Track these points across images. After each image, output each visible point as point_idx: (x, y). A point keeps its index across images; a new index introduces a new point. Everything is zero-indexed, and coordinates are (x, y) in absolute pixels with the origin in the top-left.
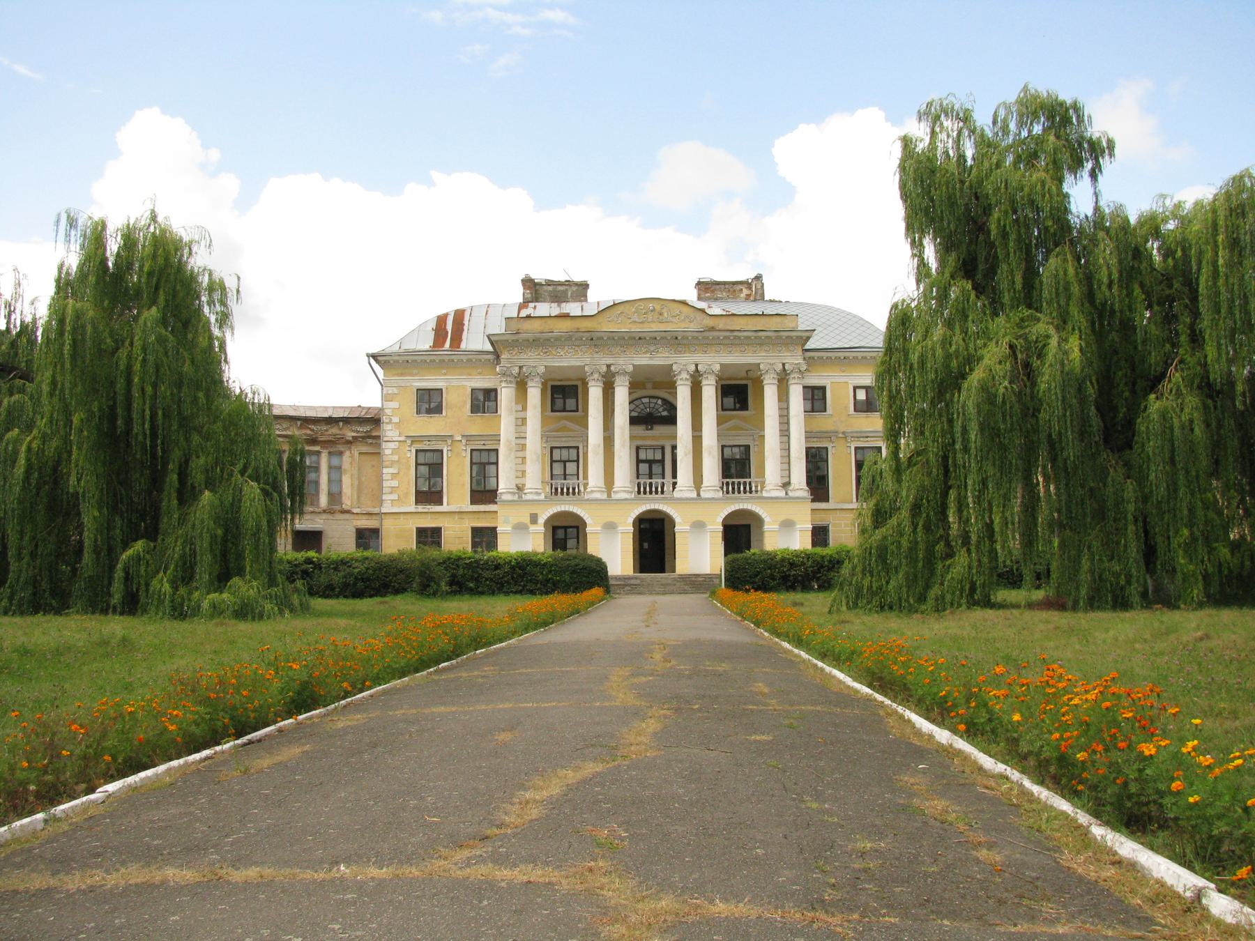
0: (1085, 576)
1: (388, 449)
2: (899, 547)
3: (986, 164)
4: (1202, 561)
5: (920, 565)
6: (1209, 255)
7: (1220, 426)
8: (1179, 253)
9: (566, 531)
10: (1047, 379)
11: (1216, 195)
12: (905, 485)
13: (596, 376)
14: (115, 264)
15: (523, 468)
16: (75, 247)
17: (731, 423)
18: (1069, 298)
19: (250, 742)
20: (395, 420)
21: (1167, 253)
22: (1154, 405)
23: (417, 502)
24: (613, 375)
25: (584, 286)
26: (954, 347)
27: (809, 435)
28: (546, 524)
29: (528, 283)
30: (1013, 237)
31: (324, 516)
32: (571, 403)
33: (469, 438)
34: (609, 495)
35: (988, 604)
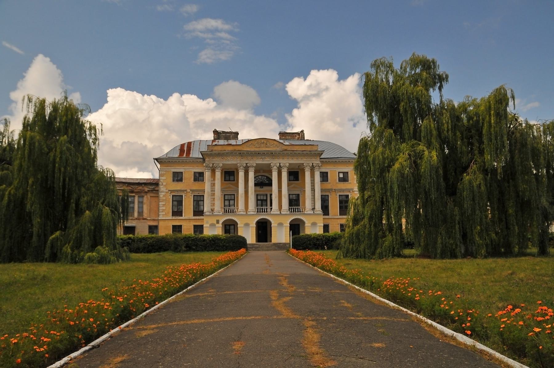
0: (439, 245)
1: (161, 195)
2: (364, 233)
3: (399, 84)
4: (485, 239)
5: (373, 240)
6: (487, 119)
7: (491, 186)
8: (475, 119)
9: (230, 226)
10: (424, 167)
11: (489, 96)
12: (366, 209)
13: (242, 168)
14: (49, 118)
15: (213, 202)
16: (32, 109)
17: (293, 185)
18: (431, 136)
19: (94, 347)
20: (164, 184)
21: (470, 118)
22: (466, 178)
24: (248, 167)
26: (386, 155)
27: (322, 190)
28: (222, 224)
29: (215, 132)
30: (409, 112)
31: (136, 221)
32: (232, 178)
33: (193, 191)
34: (247, 213)
35: (399, 256)
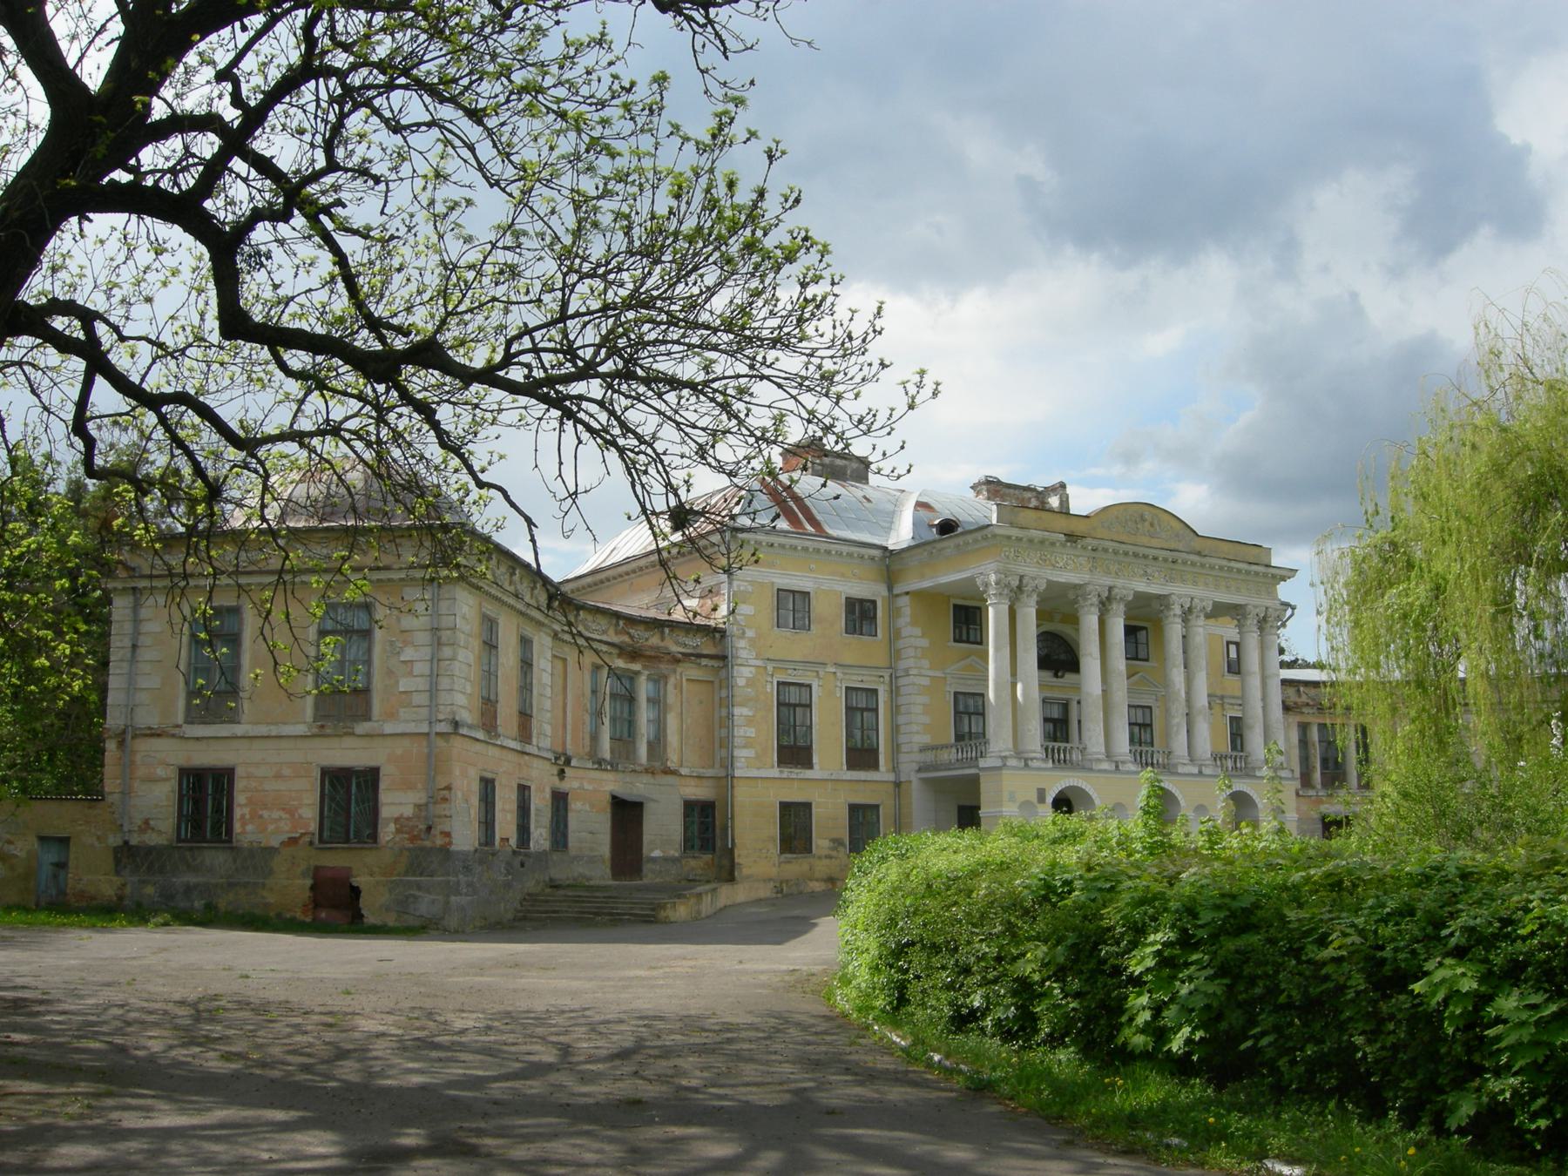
1: (742, 675)
31: (646, 778)
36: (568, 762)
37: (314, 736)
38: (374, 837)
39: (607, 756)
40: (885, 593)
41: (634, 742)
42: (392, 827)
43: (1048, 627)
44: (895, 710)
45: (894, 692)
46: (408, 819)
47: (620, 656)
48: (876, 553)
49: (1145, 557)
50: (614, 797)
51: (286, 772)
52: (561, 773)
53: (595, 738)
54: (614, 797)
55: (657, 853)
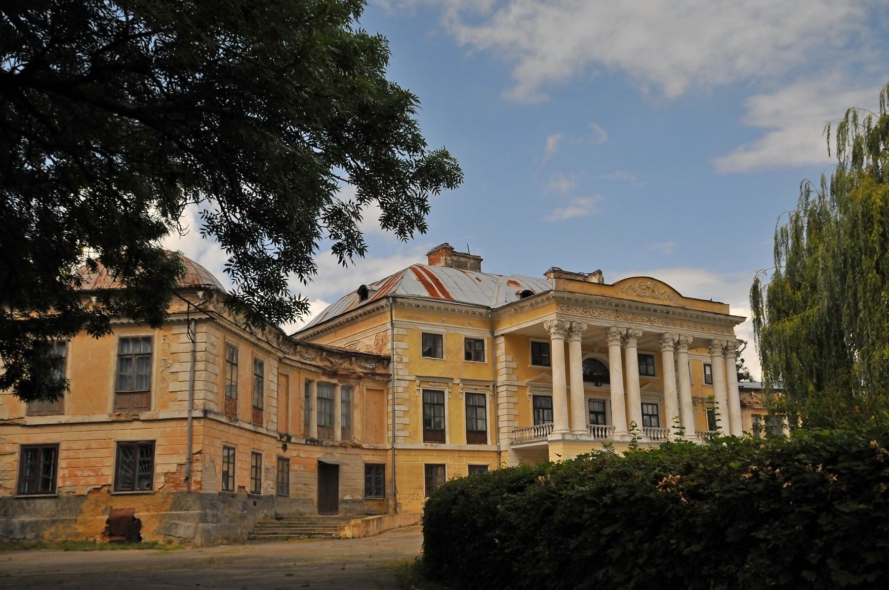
1: (400, 387)
23: (426, 439)
25: (478, 260)
31: (340, 450)
36: (289, 439)
37: (113, 422)
38: (150, 486)
39: (315, 436)
40: (489, 335)
41: (333, 428)
42: (162, 479)
43: (590, 355)
44: (496, 406)
45: (495, 395)
46: (173, 473)
47: (324, 374)
48: (484, 311)
49: (649, 310)
50: (319, 462)
51: (94, 445)
52: (285, 448)
53: (307, 425)
54: (319, 462)
55: (348, 497)
